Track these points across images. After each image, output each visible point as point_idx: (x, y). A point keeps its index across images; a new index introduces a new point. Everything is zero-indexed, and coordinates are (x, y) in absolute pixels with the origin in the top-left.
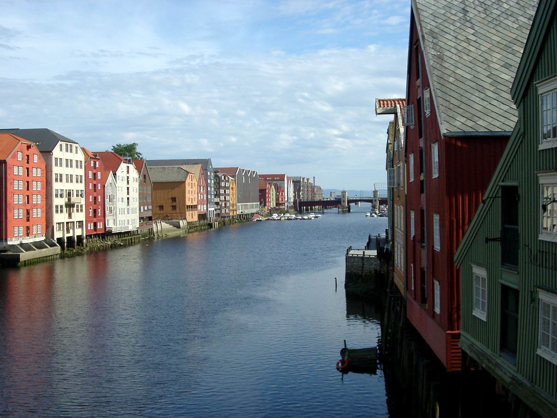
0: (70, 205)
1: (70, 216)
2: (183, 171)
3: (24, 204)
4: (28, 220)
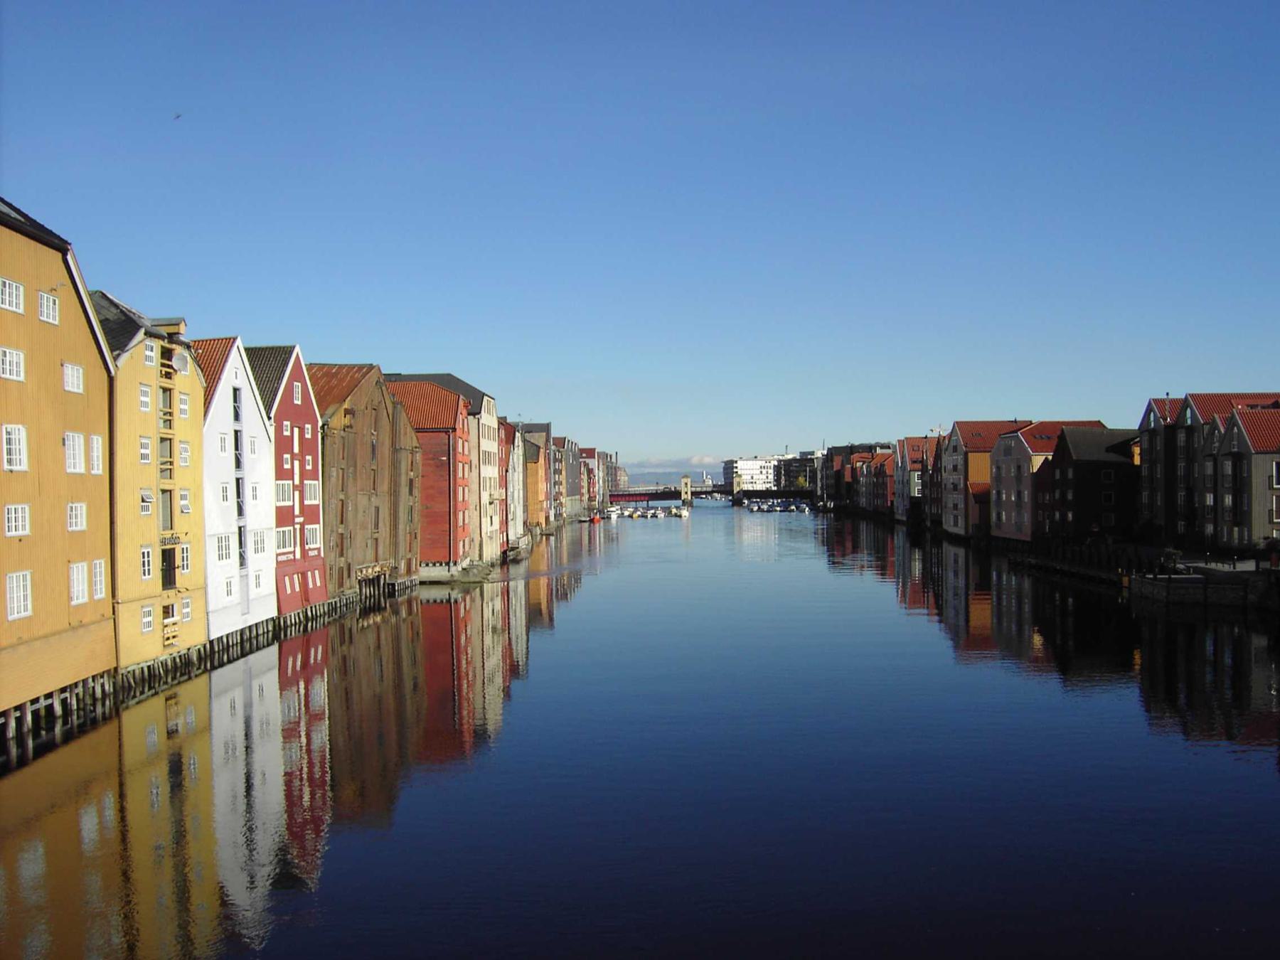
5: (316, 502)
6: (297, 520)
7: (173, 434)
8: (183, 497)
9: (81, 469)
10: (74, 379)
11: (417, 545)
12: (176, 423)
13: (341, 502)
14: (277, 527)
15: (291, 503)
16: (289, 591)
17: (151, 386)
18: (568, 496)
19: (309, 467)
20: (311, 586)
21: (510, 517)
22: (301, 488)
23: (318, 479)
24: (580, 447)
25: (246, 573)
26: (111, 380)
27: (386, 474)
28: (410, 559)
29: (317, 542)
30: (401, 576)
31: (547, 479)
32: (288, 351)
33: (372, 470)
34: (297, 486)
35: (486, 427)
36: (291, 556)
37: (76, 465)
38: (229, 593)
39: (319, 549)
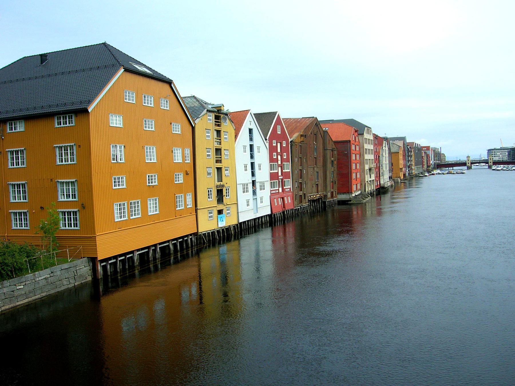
0: (370, 169)
1: (370, 178)
2: (396, 145)
5: (289, 171)
6: (280, 178)
7: (222, 147)
8: (226, 170)
9: (180, 161)
10: (177, 129)
11: (336, 187)
12: (222, 143)
13: (300, 171)
14: (270, 181)
15: (277, 171)
16: (276, 205)
17: (210, 130)
18: (415, 166)
19: (285, 157)
20: (286, 202)
21: (381, 175)
22: (282, 167)
23: (289, 162)
24: (421, 146)
25: (256, 198)
26: (193, 128)
27: (321, 159)
28: (333, 192)
29: (288, 186)
30: (328, 198)
31: (404, 159)
32: (274, 113)
33: (315, 158)
34: (280, 165)
35: (367, 140)
36: (277, 191)
37: (178, 159)
38: (248, 205)
39: (290, 188)
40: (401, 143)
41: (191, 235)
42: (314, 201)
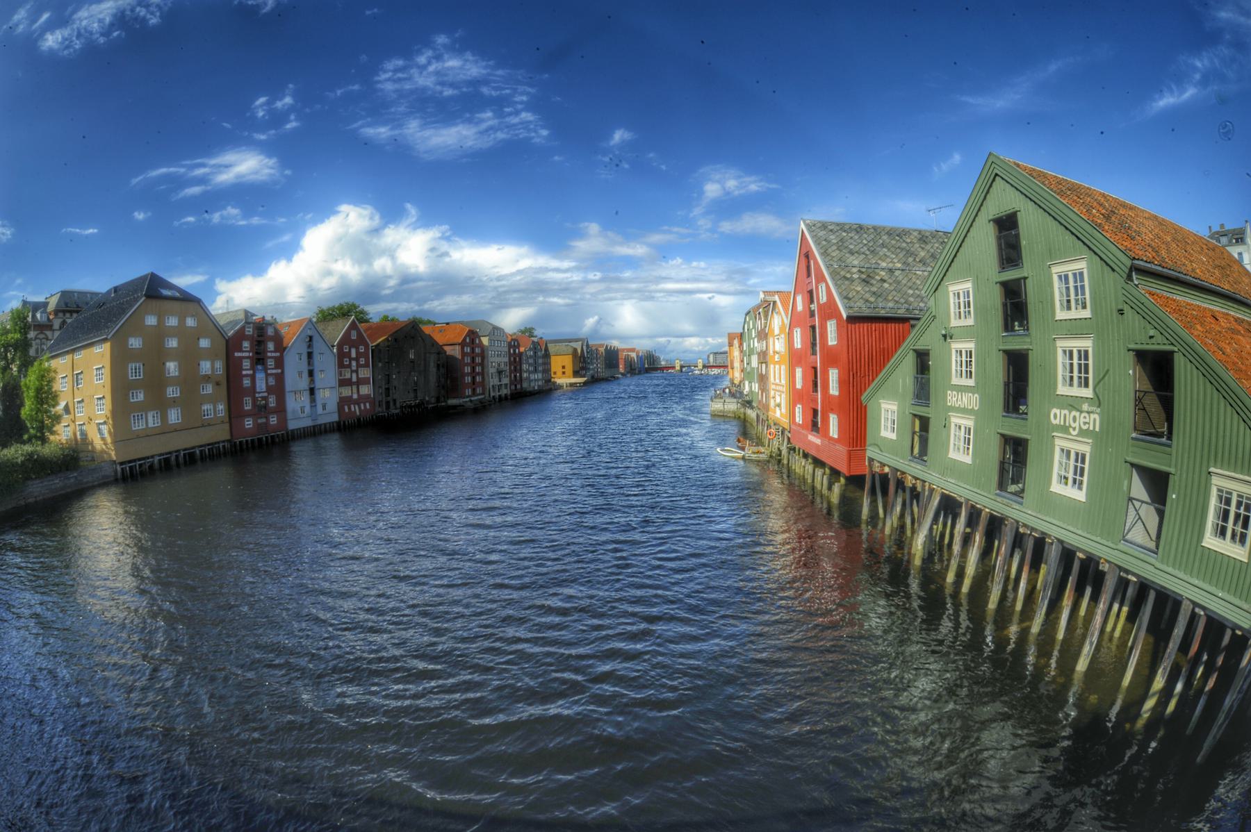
0: (500, 372)
3: (471, 373)
4: (474, 384)
20: (363, 408)
22: (357, 371)
38: (303, 412)
40: (578, 346)
41: (223, 442)
42: (410, 406)
